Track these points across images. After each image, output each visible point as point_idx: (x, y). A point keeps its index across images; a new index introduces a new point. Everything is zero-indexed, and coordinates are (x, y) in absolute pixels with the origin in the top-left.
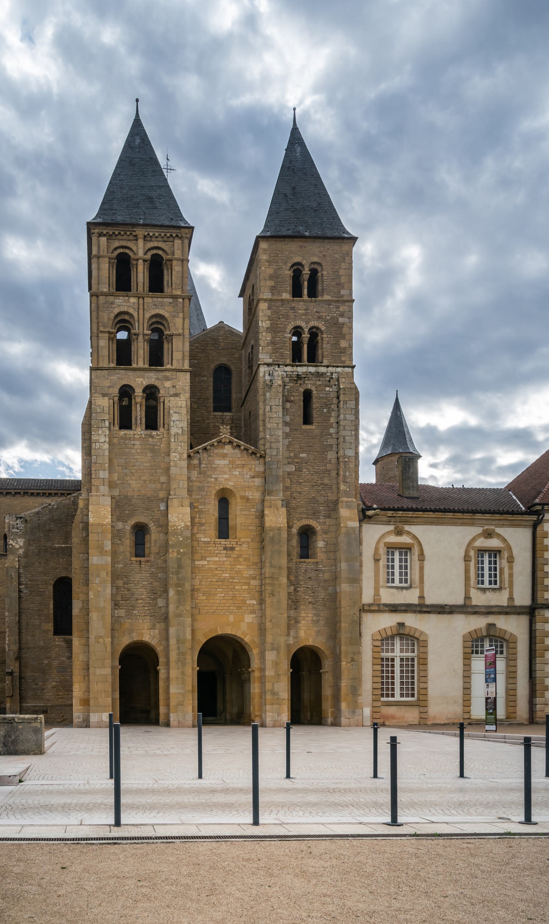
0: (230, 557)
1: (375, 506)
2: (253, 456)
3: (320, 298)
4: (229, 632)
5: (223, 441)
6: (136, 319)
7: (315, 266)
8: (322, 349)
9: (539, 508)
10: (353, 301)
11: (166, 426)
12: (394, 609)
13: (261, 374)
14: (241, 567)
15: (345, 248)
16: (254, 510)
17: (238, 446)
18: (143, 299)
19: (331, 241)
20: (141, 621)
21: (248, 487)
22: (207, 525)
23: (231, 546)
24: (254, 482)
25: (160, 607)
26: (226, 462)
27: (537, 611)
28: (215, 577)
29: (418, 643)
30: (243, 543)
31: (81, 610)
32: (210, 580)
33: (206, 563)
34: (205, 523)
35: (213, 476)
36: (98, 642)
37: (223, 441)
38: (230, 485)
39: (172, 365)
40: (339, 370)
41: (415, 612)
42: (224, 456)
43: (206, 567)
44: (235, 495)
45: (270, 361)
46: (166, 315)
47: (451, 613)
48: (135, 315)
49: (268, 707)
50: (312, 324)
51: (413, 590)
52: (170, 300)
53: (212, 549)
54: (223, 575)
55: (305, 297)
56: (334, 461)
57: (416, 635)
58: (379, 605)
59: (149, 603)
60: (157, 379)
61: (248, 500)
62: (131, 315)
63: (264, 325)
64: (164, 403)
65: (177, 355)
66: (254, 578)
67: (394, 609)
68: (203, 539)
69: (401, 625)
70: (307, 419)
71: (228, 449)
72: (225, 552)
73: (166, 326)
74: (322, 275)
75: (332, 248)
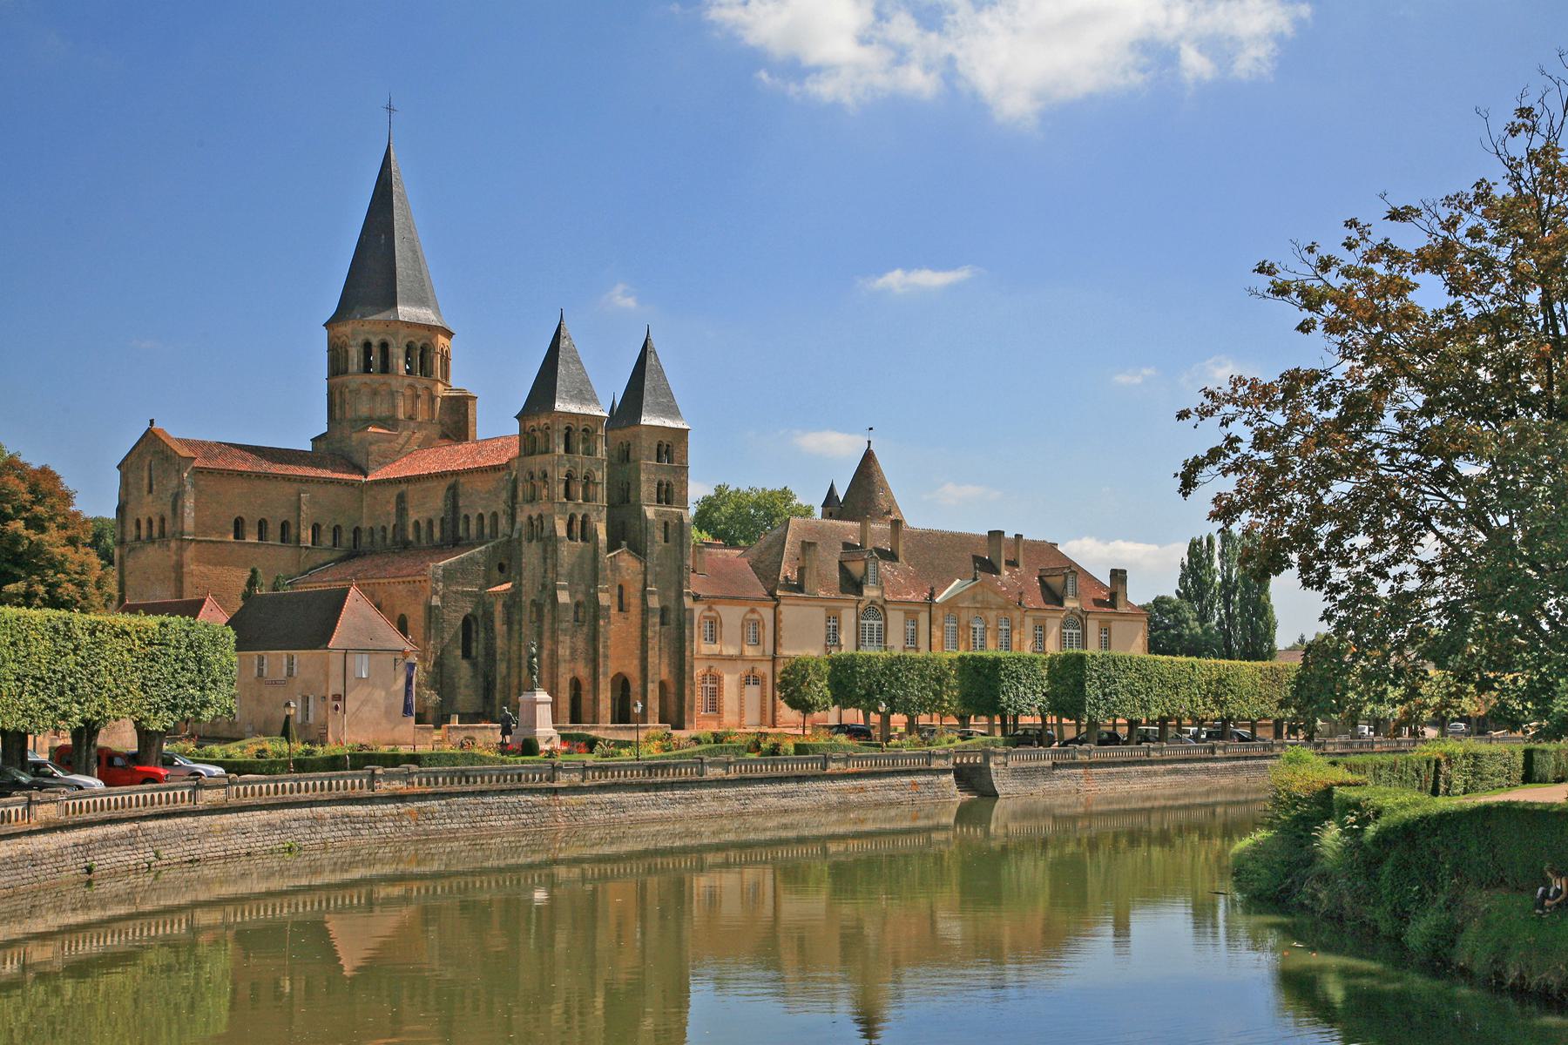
65: (599, 496)
67: (709, 657)
71: (626, 556)
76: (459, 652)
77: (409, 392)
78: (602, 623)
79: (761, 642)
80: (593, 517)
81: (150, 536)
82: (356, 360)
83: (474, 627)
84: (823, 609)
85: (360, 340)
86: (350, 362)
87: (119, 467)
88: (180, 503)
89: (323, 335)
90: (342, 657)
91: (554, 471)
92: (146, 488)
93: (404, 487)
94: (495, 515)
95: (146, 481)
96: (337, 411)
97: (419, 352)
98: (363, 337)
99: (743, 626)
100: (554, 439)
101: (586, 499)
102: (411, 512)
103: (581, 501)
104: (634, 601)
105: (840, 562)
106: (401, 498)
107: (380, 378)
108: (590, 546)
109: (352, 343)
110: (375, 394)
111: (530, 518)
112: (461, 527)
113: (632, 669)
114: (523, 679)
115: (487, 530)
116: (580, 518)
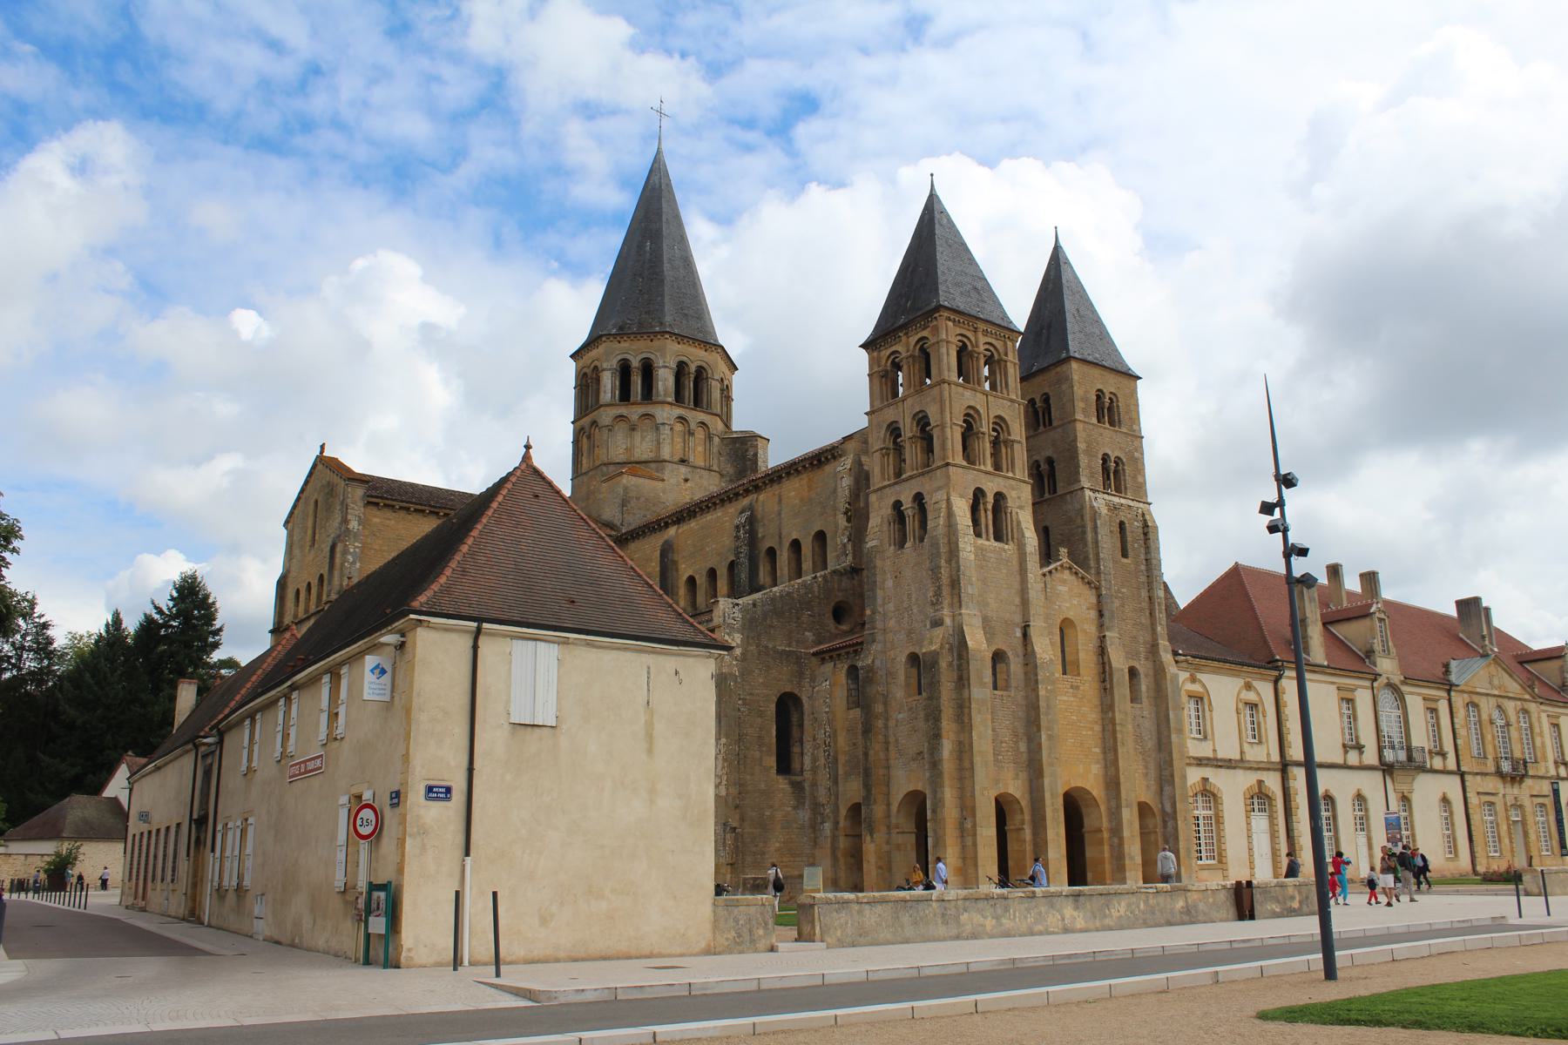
0: (1075, 696)
1: (1180, 652)
2: (1088, 586)
3: (1117, 429)
4: (1079, 784)
6: (983, 417)
7: (1112, 396)
8: (1125, 480)
9: (1280, 664)
10: (1143, 437)
11: (1016, 540)
12: (1200, 762)
13: (1087, 498)
15: (1132, 382)
17: (1076, 573)
18: (987, 396)
19: (1123, 375)
20: (1006, 769)
21: (1086, 619)
25: (1022, 753)
26: (1066, 589)
27: (1289, 767)
29: (1214, 799)
31: (951, 752)
35: (1057, 603)
36: (983, 795)
37: (1065, 565)
38: (1071, 615)
39: (1013, 472)
40: (1141, 505)
41: (1212, 766)
42: (1064, 582)
46: (1007, 418)
47: (1235, 768)
48: (981, 411)
49: (1128, 874)
50: (1117, 453)
51: (1209, 742)
52: (1009, 403)
53: (1060, 686)
55: (1107, 425)
56: (1147, 599)
57: (1216, 792)
58: (1189, 758)
59: (1012, 747)
60: (1005, 487)
61: (1087, 633)
62: (977, 411)
64: (1011, 513)
66: (1096, 722)
67: (1200, 762)
69: (1205, 780)
70: (1125, 554)
71: (1066, 575)
72: (1071, 690)
73: (1005, 428)
74: (1118, 406)
75: (1124, 381)
76: (772, 761)
77: (679, 427)
78: (1042, 693)
79: (1264, 740)
80: (1012, 496)
81: (306, 611)
82: (609, 386)
83: (795, 719)
84: (1334, 687)
85: (614, 363)
86: (602, 389)
87: (286, 524)
88: (339, 548)
89: (570, 370)
90: (469, 642)
91: (942, 411)
92: (308, 544)
93: (672, 531)
94: (821, 537)
95: (310, 532)
96: (584, 462)
97: (692, 379)
98: (619, 357)
99: (1238, 713)
100: (940, 361)
101: (997, 467)
102: (683, 566)
103: (989, 468)
104: (1086, 656)
105: (1324, 624)
106: (667, 550)
107: (642, 410)
108: (1010, 548)
109: (605, 365)
110: (633, 429)
111: (897, 505)
112: (761, 568)
113: (1089, 779)
114: (894, 807)
115: (807, 564)
116: (990, 499)
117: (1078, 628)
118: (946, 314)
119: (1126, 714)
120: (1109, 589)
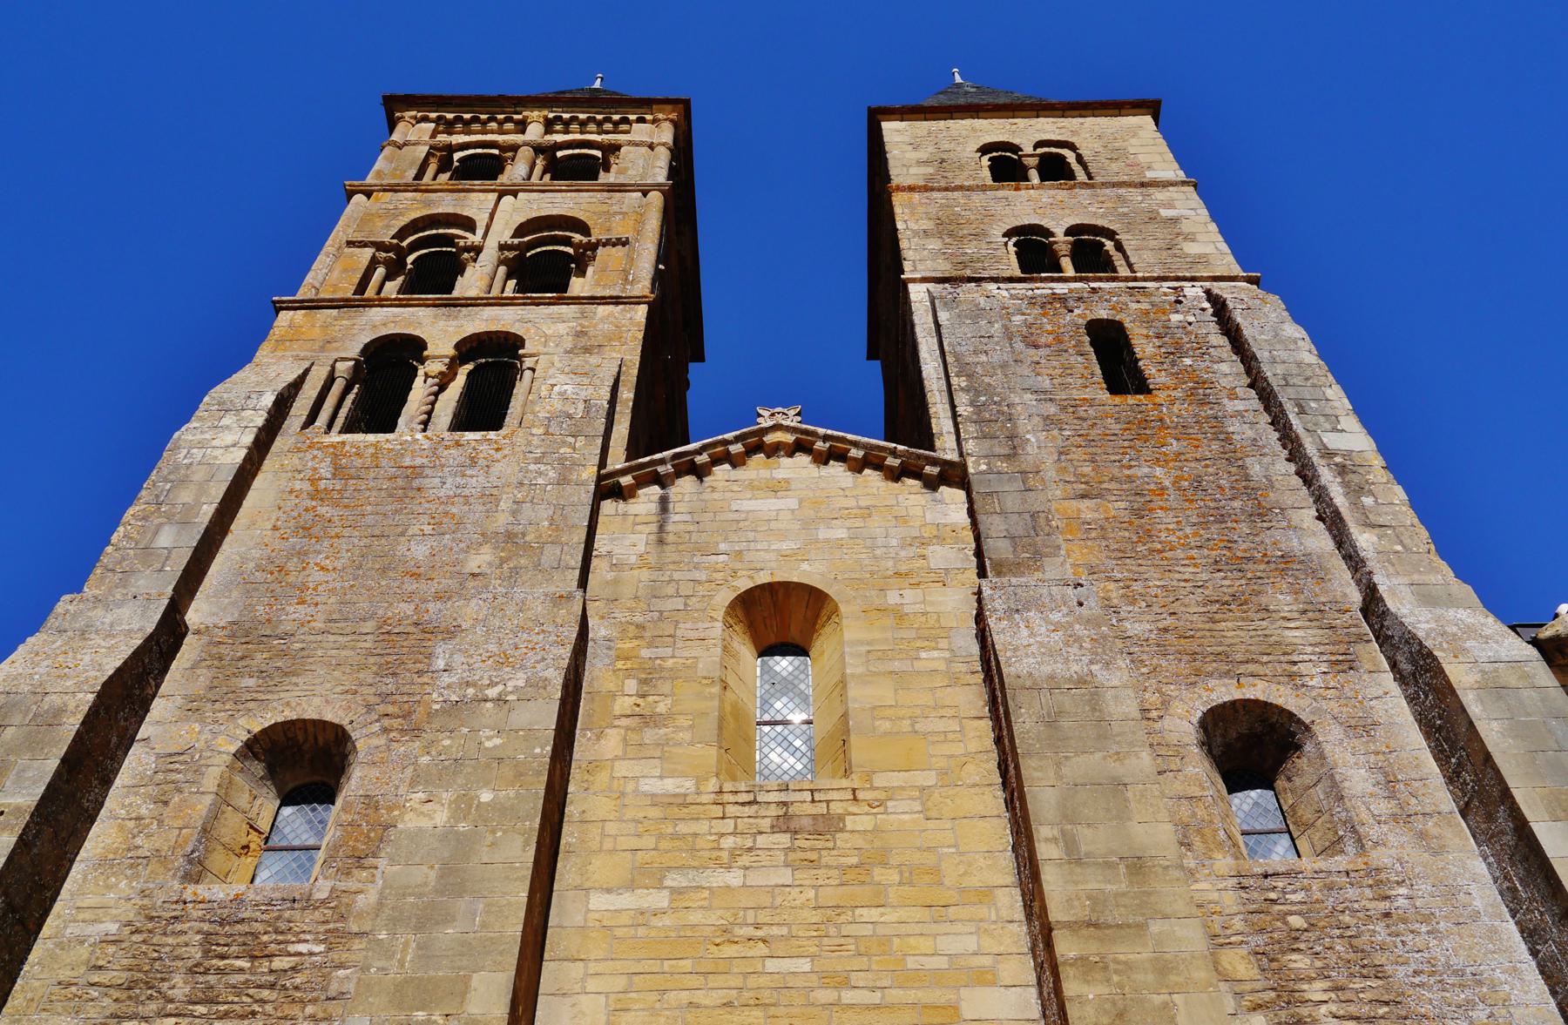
5: (770, 438)
14: (891, 916)
16: (936, 654)
22: (683, 721)
23: (822, 809)
24: (924, 557)
28: (714, 981)
30: (891, 793)
32: (685, 997)
33: (660, 899)
34: (670, 715)
42: (777, 488)
43: (667, 921)
44: (836, 610)
45: (943, 268)
54: (771, 965)
63: (912, 225)
66: (985, 978)
68: (651, 785)
72: (784, 839)
117: (843, 608)
118: (414, 113)
119: (1138, 866)
120: (1011, 457)
